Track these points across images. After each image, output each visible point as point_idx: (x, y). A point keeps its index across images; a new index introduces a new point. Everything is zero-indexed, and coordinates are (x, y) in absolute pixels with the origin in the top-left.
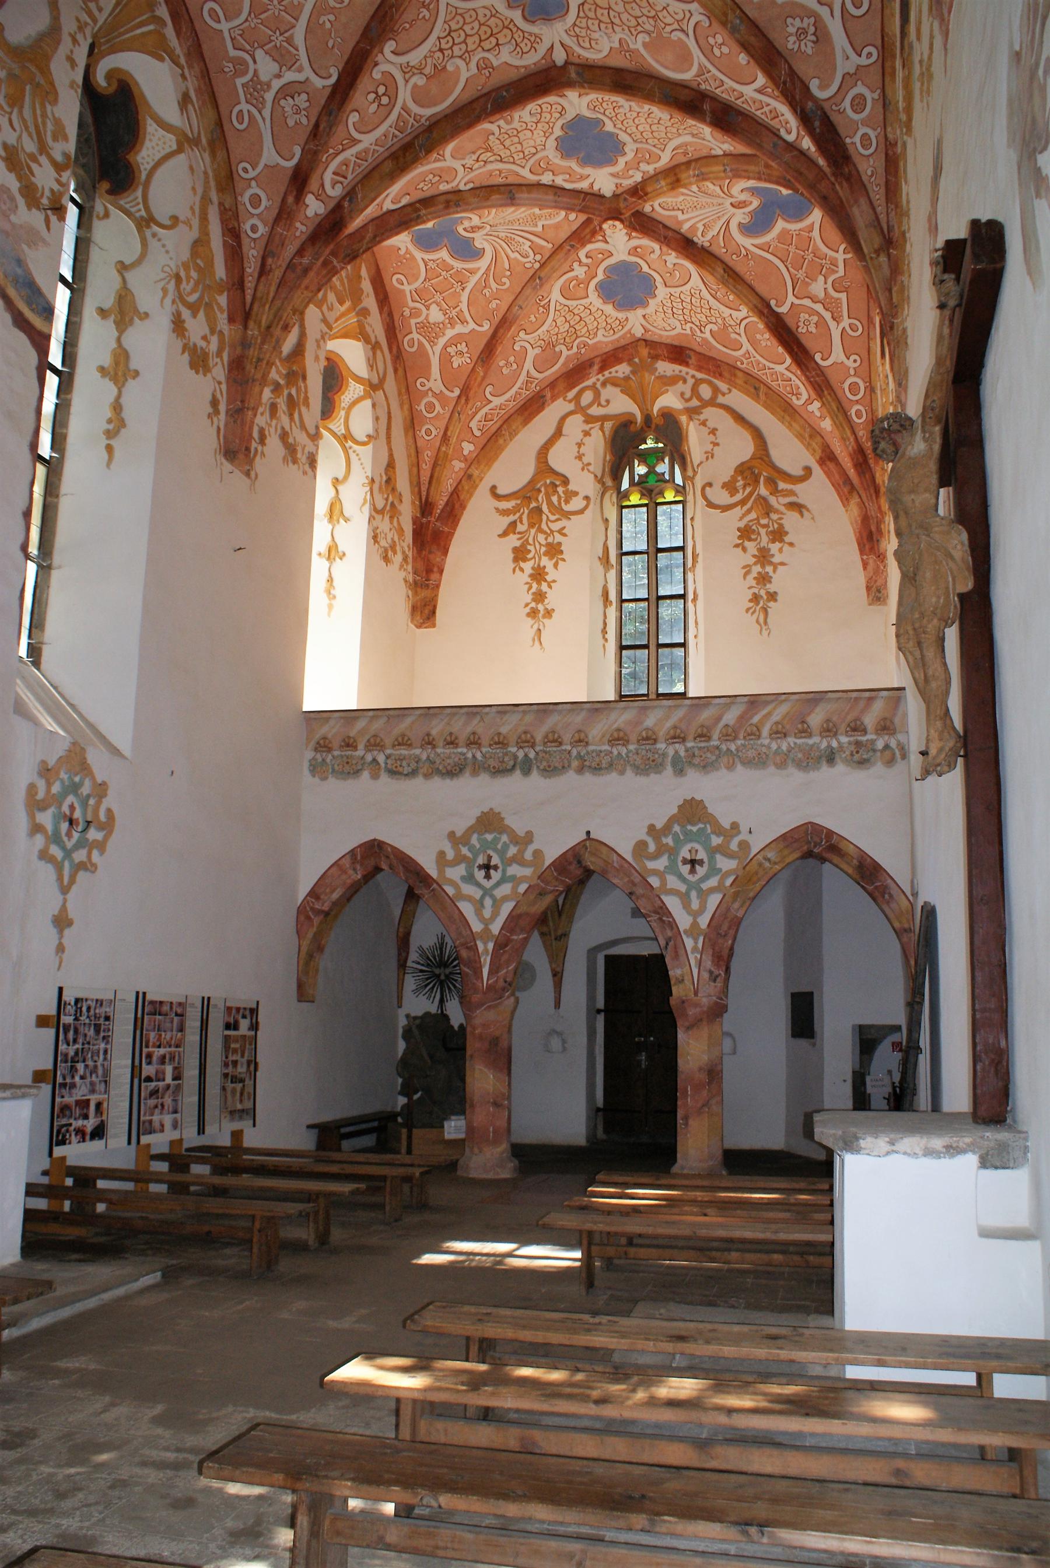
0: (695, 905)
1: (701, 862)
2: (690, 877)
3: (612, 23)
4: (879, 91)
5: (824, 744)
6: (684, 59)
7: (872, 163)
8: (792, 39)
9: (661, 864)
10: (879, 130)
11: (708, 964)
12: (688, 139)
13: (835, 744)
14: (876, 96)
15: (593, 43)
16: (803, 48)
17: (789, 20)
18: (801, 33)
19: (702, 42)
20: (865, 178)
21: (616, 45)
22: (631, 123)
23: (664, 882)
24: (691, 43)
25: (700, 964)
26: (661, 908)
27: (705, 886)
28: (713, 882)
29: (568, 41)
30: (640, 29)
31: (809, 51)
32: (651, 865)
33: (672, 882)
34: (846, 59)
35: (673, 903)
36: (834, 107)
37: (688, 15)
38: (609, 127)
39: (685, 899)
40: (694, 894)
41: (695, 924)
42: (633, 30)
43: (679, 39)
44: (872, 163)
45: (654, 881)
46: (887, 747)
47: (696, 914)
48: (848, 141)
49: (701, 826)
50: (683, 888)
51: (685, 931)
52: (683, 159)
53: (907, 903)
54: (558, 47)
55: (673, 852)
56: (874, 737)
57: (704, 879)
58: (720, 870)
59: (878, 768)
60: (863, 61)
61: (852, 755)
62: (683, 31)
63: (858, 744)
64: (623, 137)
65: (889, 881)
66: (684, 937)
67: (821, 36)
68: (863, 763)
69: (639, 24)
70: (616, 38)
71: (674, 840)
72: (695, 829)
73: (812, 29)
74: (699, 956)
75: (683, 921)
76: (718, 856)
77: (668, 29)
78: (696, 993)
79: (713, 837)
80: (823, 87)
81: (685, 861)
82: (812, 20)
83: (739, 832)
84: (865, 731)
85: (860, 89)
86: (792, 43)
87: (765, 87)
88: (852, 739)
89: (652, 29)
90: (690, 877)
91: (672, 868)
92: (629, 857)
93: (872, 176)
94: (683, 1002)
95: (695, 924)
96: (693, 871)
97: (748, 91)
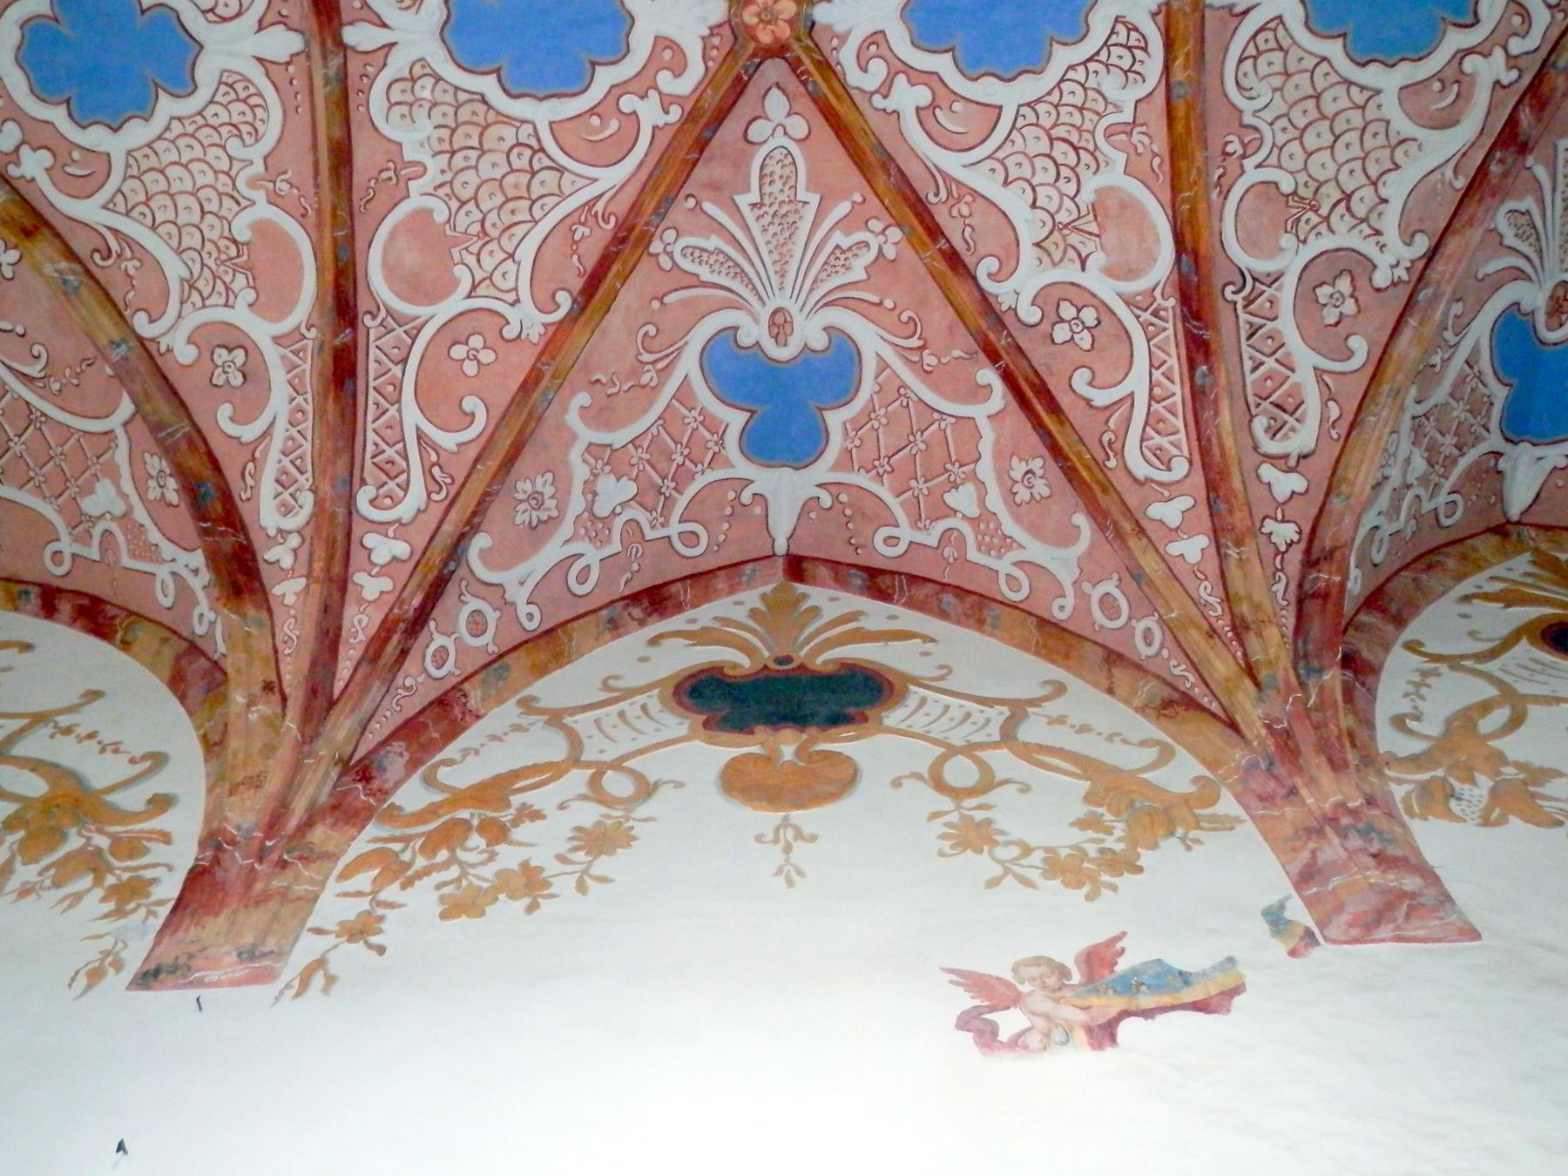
3: (453, 153)
4: (496, 649)
6: (427, 290)
7: (420, 679)
8: (528, 487)
10: (457, 672)
12: (174, 269)
14: (492, 648)
15: (405, 109)
16: (521, 507)
17: (549, 476)
18: (537, 499)
19: (465, 326)
20: (399, 680)
21: (409, 155)
22: (198, 152)
24: (455, 303)
29: (398, 63)
30: (454, 204)
31: (519, 519)
34: (520, 581)
36: (464, 583)
37: (511, 297)
38: (167, 106)
42: (447, 189)
43: (455, 283)
44: (420, 679)
48: (432, 624)
52: (81, 246)
54: (383, 37)
60: (523, 610)
62: (474, 287)
64: (137, 133)
67: (540, 531)
69: (463, 203)
70: (424, 156)
73: (544, 517)
77: (471, 260)
80: (483, 553)
82: (555, 513)
85: (492, 616)
86: (525, 487)
87: (436, 448)
89: (461, 227)
93: (405, 688)
97: (412, 416)
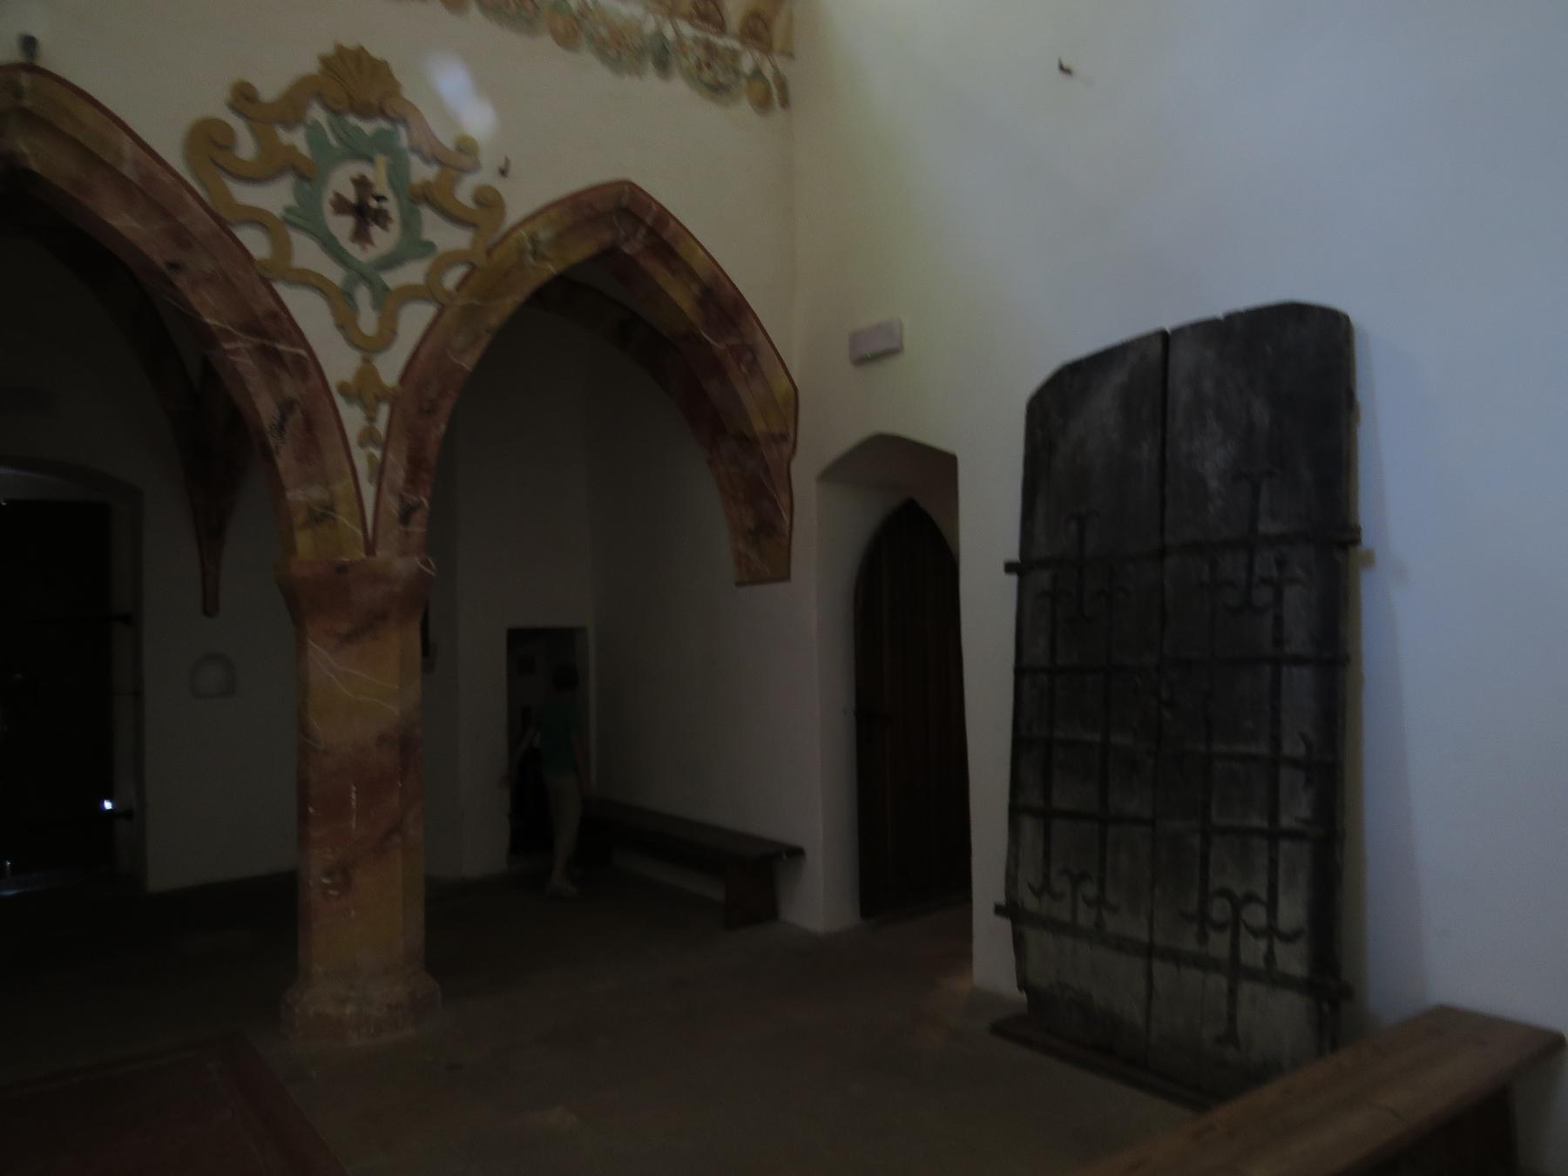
0: (368, 321)
1: (381, 218)
2: (354, 250)
5: (650, 26)
9: (275, 197)
11: (398, 475)
13: (669, 33)
23: (282, 247)
25: (379, 472)
26: (274, 316)
27: (395, 279)
28: (413, 273)
32: (246, 195)
33: (306, 253)
35: (309, 312)
39: (341, 304)
40: (363, 295)
41: (367, 373)
45: (255, 242)
46: (757, 73)
47: (370, 347)
49: (383, 124)
50: (335, 274)
51: (344, 389)
53: (785, 380)
55: (306, 175)
56: (736, 45)
57: (391, 261)
58: (430, 246)
59: (743, 109)
61: (699, 67)
63: (709, 47)
65: (761, 336)
66: (340, 401)
68: (717, 90)
71: (310, 143)
72: (368, 127)
74: (377, 453)
75: (338, 362)
76: (427, 214)
78: (370, 548)
79: (415, 161)
81: (341, 206)
83: (476, 167)
84: (721, 28)
88: (699, 34)
90: (354, 250)
91: (305, 218)
92: (174, 156)
94: (342, 569)
95: (367, 373)
96: (361, 235)
